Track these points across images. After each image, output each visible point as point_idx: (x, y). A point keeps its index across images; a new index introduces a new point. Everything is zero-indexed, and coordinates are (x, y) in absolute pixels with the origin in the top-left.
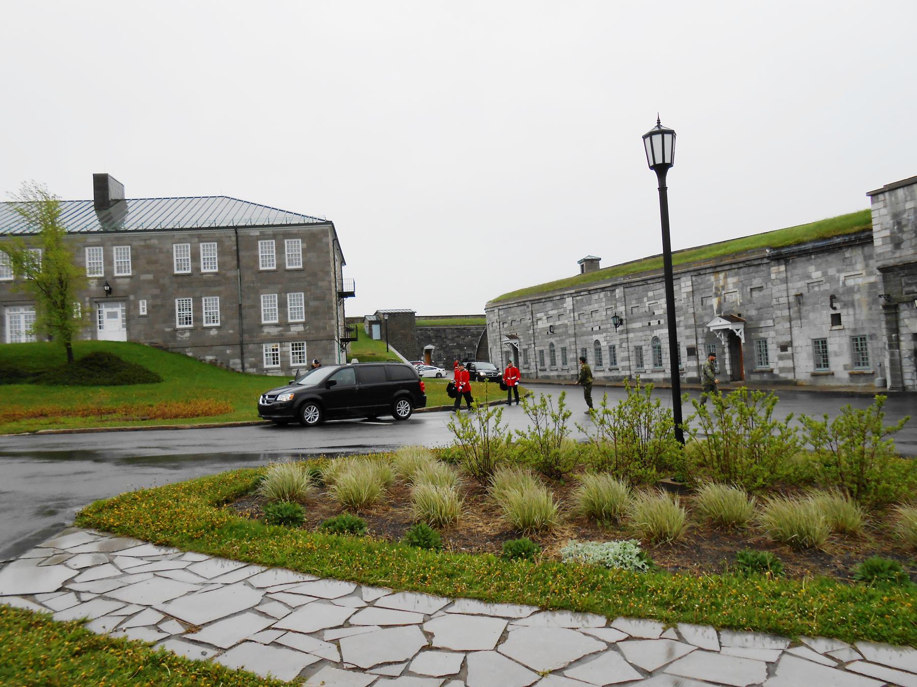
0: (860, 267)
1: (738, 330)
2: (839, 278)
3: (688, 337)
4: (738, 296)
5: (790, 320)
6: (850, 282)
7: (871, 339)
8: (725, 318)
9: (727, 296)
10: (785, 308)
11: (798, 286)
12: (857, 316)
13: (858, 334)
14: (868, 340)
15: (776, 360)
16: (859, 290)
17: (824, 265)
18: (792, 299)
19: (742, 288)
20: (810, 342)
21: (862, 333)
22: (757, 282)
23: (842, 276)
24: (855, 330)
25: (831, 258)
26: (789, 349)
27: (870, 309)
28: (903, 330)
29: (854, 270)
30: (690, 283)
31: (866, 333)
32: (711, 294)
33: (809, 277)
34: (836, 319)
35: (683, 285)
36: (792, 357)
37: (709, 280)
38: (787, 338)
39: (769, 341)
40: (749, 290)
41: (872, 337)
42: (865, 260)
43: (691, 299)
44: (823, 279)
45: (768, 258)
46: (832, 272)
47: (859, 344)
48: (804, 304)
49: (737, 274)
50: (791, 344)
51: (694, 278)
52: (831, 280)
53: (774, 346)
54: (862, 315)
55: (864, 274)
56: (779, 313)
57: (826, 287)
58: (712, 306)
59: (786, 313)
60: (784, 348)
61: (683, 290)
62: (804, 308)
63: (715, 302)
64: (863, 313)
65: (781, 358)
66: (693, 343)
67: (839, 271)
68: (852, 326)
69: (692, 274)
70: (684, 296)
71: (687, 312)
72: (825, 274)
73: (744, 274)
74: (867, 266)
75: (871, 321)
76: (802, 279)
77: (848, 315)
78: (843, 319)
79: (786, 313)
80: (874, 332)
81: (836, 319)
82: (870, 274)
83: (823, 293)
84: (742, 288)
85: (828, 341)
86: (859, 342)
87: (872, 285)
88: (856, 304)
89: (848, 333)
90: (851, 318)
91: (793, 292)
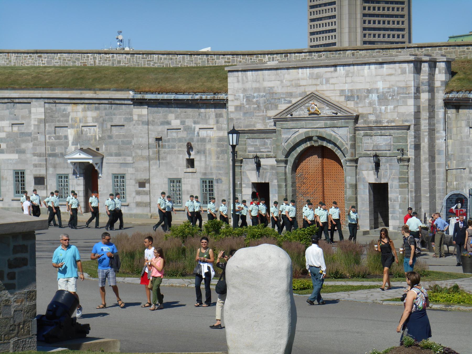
0: (212, 122)
1: (96, 164)
2: (195, 128)
3: (35, 166)
4: (97, 129)
5: (149, 159)
6: (203, 134)
7: (218, 183)
8: (81, 149)
9: (85, 129)
10: (145, 148)
11: (158, 130)
12: (208, 163)
13: (207, 177)
14: (215, 183)
15: (134, 194)
16: (210, 141)
17: (183, 115)
18: (152, 141)
19: (102, 124)
20: (166, 181)
21: (210, 177)
22: (117, 120)
23: (198, 127)
24: (205, 174)
25: (189, 110)
26: (147, 185)
27: (218, 158)
28: (245, 181)
29: (207, 123)
30: (42, 110)
31: (214, 177)
32: (66, 124)
33: (169, 123)
34: (191, 163)
35: (33, 110)
36: (148, 193)
37: (64, 110)
38: (143, 176)
39: (127, 177)
40: (109, 127)
41: (218, 180)
42: (216, 117)
43: (42, 125)
44: (181, 127)
45: (132, 100)
46: (189, 122)
47: (208, 186)
48: (163, 147)
49: (97, 109)
50: (148, 181)
51: (47, 105)
52: (188, 129)
53: (133, 182)
54: (212, 162)
55: (215, 128)
56: (139, 152)
57: (183, 134)
58: (66, 137)
59: (145, 153)
60: (142, 185)
61: (33, 116)
62: (162, 150)
63: (71, 133)
64: (213, 161)
65: (138, 193)
66: (41, 172)
67: (195, 123)
68: (203, 171)
69: (46, 101)
70: (33, 122)
71: (36, 139)
72: (183, 123)
73: (105, 109)
74: (217, 122)
75: (218, 168)
76: (163, 123)
77: (200, 161)
78: (196, 163)
79: (145, 153)
80: (220, 177)
81: (191, 163)
82: (220, 129)
83: (180, 140)
84: (103, 123)
85: (183, 180)
86: (208, 184)
87: (220, 139)
88: (207, 152)
89: (199, 176)
90: (203, 164)
91: (154, 135)
